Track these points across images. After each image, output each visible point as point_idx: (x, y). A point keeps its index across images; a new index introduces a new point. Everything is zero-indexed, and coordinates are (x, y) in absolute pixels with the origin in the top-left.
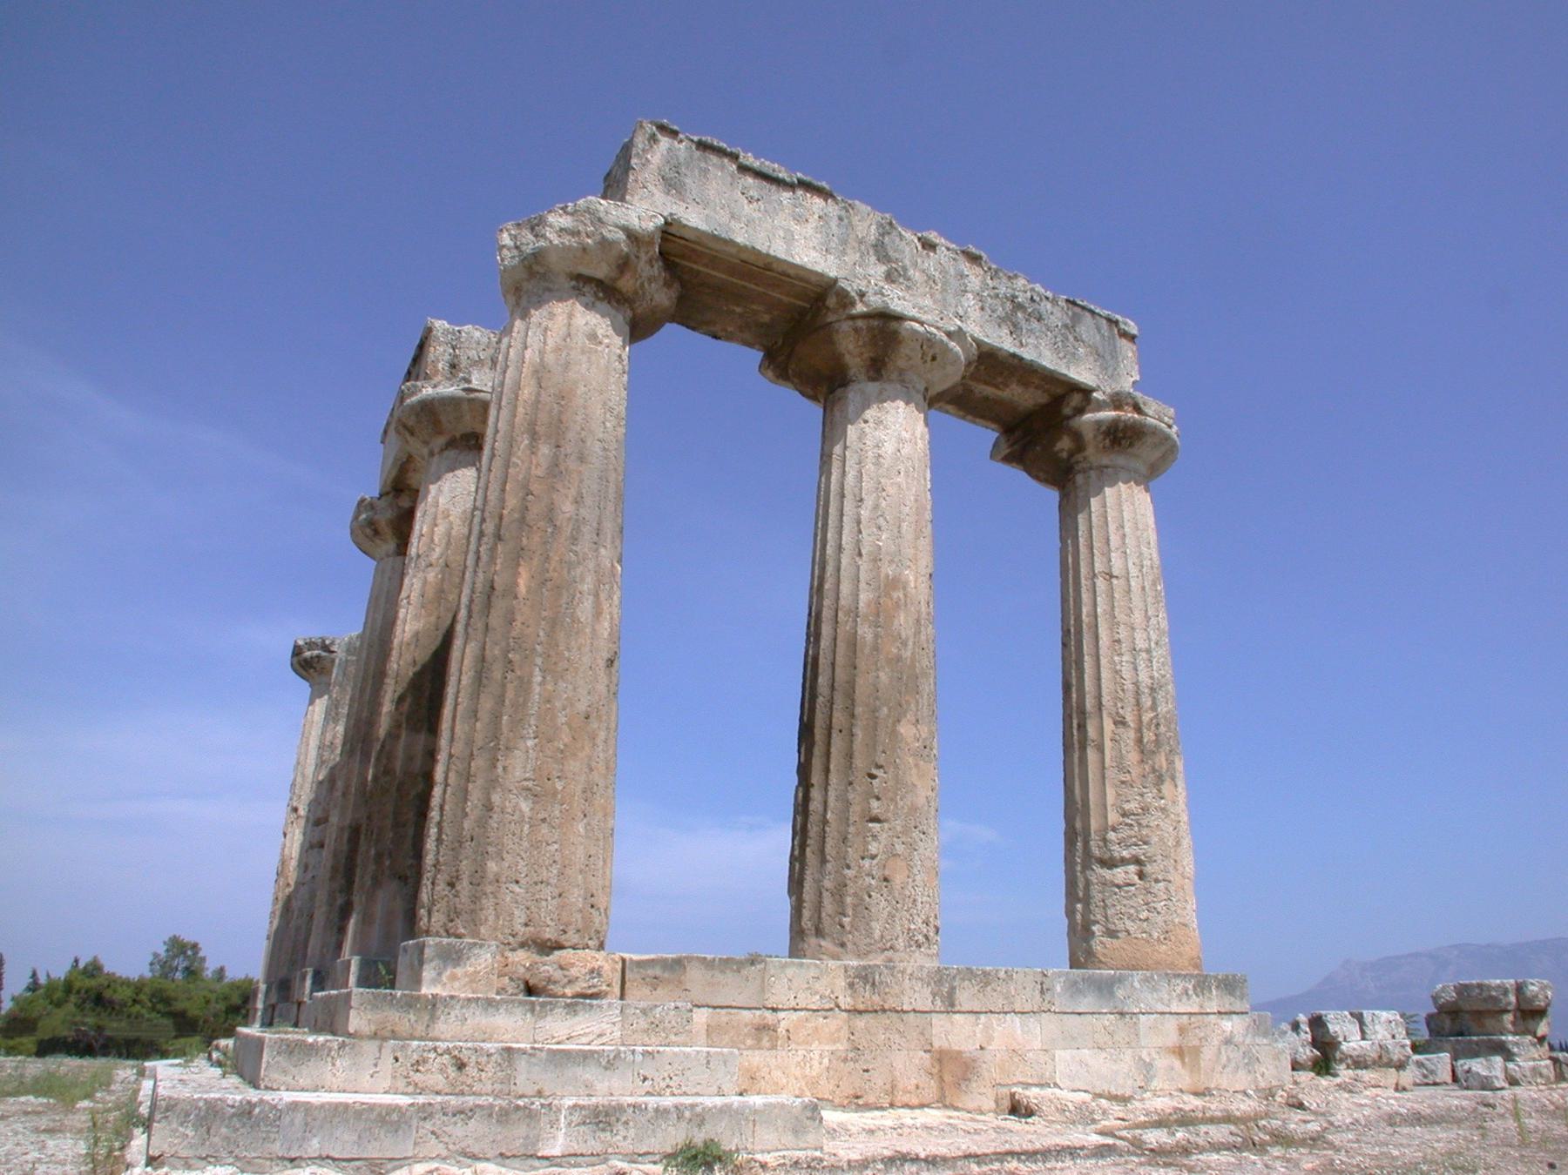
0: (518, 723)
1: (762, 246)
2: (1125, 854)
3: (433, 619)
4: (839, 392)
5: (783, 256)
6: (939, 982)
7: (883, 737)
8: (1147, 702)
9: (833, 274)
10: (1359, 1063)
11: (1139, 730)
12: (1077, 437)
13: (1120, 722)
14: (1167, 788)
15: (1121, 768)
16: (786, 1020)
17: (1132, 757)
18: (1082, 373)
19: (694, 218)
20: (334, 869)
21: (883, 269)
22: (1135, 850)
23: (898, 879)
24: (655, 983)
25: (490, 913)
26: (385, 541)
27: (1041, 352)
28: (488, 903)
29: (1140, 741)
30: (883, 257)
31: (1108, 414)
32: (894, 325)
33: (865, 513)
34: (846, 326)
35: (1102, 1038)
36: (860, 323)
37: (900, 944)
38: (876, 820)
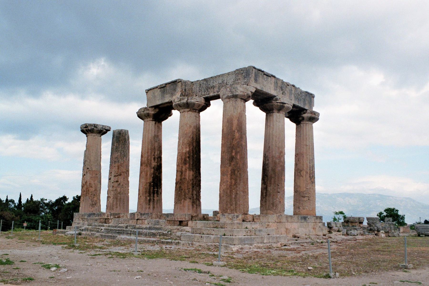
0: (240, 180)
1: (267, 91)
2: (307, 196)
3: (191, 148)
4: (271, 114)
5: (270, 93)
6: (287, 218)
7: (280, 179)
8: (311, 169)
9: (276, 95)
12: (303, 119)
13: (307, 173)
16: (270, 224)
17: (309, 179)
18: (306, 108)
19: (259, 88)
20: (146, 192)
21: (282, 92)
23: (282, 201)
26: (150, 118)
27: (301, 105)
29: (310, 176)
30: (282, 90)
31: (309, 115)
32: (284, 105)
33: (277, 139)
34: (276, 104)
35: (304, 226)
36: (279, 104)
38: (279, 192)
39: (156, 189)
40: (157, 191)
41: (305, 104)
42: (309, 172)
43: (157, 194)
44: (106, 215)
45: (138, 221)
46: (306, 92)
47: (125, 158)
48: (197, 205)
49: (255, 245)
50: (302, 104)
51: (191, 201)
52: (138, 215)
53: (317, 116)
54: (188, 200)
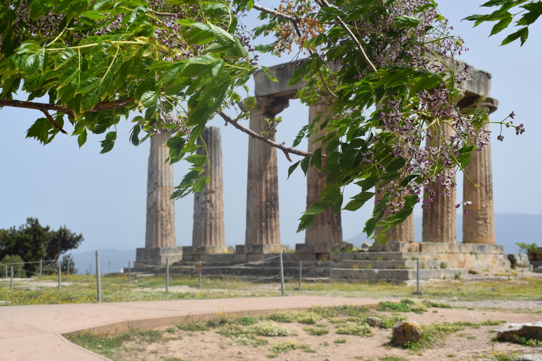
2: (482, 217)
8: (488, 180)
10: (519, 266)
11: (486, 187)
13: (481, 185)
14: (491, 201)
15: (481, 195)
18: (481, 93)
22: (484, 216)
23: (453, 225)
24: (425, 248)
25: (403, 236)
27: (475, 91)
28: (403, 234)
29: (486, 190)
37: (453, 239)
39: (273, 212)
40: (275, 213)
41: (479, 89)
42: (484, 184)
43: (275, 218)
44: (195, 249)
45: (250, 256)
46: (481, 72)
47: (217, 167)
48: (338, 232)
49: (432, 280)
50: (476, 89)
51: (331, 226)
52: (249, 248)
53: (495, 105)
54: (327, 225)
